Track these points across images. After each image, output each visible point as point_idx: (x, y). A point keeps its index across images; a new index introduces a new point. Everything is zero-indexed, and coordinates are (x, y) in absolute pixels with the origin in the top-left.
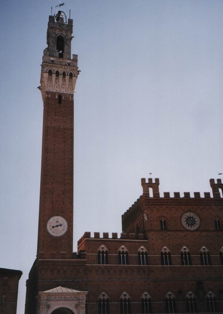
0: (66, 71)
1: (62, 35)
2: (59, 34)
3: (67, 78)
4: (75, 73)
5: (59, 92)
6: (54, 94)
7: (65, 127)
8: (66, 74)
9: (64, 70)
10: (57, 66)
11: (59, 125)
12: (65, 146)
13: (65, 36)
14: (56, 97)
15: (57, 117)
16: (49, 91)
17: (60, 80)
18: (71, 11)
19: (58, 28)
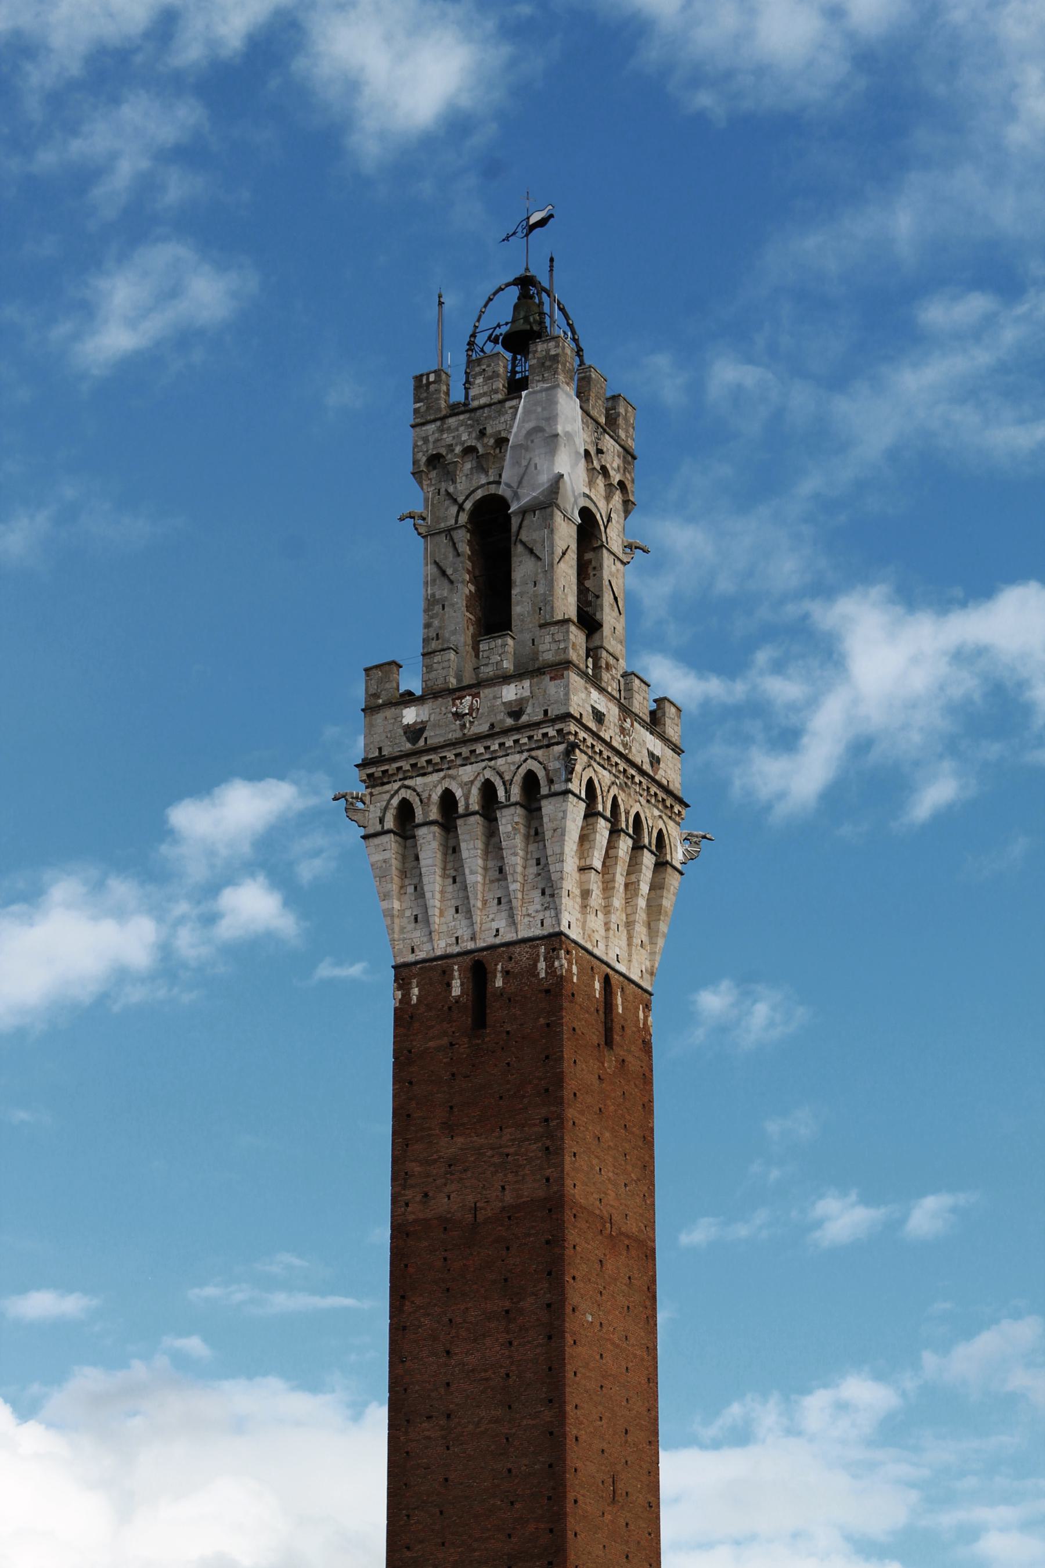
0: (501, 775)
1: (492, 489)
2: (482, 486)
3: (510, 821)
4: (554, 765)
5: (470, 946)
6: (444, 972)
7: (509, 1198)
8: (501, 793)
9: (488, 774)
10: (443, 758)
11: (470, 1199)
12: (511, 1343)
13: (515, 485)
14: (456, 991)
15: (459, 1140)
16: (411, 958)
17: (465, 854)
18: (555, 263)
19: (469, 450)
